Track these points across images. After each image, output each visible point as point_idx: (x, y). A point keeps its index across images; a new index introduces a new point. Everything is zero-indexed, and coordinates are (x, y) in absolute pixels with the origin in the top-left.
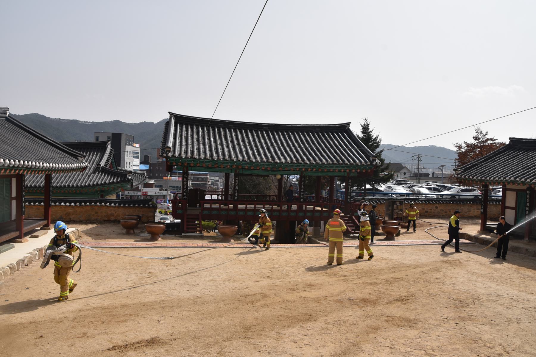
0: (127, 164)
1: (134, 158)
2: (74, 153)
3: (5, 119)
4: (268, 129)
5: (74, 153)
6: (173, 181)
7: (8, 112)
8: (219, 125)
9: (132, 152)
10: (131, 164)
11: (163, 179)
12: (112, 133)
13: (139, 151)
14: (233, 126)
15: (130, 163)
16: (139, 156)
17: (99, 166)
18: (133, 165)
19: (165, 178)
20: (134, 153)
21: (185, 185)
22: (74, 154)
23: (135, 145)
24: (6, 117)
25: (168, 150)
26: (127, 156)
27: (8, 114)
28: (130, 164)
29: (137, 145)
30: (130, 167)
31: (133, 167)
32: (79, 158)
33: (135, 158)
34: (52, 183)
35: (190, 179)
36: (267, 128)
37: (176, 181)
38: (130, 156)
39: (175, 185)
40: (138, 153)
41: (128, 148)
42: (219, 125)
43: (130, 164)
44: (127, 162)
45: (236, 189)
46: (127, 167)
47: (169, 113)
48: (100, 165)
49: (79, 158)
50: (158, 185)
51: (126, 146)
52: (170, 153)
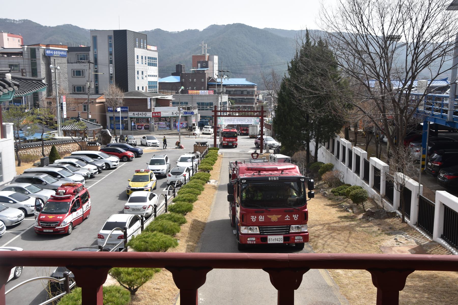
0: (138, 73)
1: (148, 65)
6: (201, 96)
9: (146, 57)
10: (145, 74)
11: (188, 93)
12: (115, 31)
13: (157, 57)
15: (142, 72)
16: (157, 63)
18: (149, 76)
19: (190, 92)
20: (148, 57)
23: (149, 47)
26: (138, 63)
28: (142, 74)
29: (154, 48)
30: (143, 78)
33: (151, 65)
37: (205, 96)
38: (142, 63)
39: (206, 101)
40: (156, 59)
41: (138, 52)
43: (142, 74)
44: (138, 72)
50: (176, 101)
51: (135, 48)
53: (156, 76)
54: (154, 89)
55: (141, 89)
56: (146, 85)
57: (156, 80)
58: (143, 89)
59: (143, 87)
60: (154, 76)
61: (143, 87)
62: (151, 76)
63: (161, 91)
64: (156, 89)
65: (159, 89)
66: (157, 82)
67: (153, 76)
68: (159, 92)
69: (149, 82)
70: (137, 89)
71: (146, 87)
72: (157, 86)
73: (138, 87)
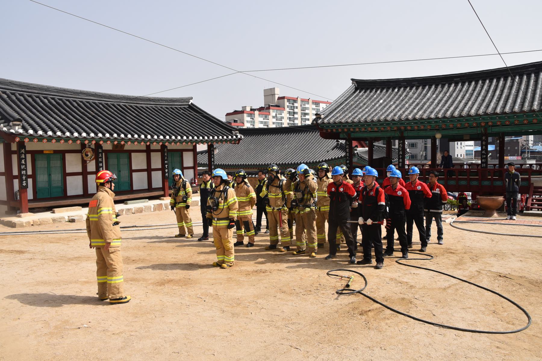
2: (230, 128)
3: (188, 106)
4: (460, 80)
5: (230, 128)
7: (191, 100)
8: (402, 84)
14: (417, 83)
17: (338, 142)
18: (466, 146)
21: (348, 152)
22: (230, 129)
24: (189, 105)
25: (319, 117)
27: (190, 103)
30: (461, 148)
31: (466, 147)
32: (233, 132)
34: (213, 154)
35: (527, 157)
36: (459, 79)
42: (402, 84)
45: (400, 155)
46: (458, 148)
47: (352, 80)
48: (339, 142)
49: (233, 132)
52: (321, 120)
53: (472, 146)
54: (470, 156)
55: (459, 156)
56: (464, 153)
57: (472, 149)
58: (461, 156)
59: (461, 155)
60: (471, 146)
61: (461, 155)
62: (468, 146)
63: (477, 158)
64: (472, 156)
65: (475, 156)
66: (473, 150)
67: (469, 146)
68: (475, 158)
69: (466, 150)
70: (456, 156)
71: (464, 155)
72: (473, 154)
73: (457, 155)
